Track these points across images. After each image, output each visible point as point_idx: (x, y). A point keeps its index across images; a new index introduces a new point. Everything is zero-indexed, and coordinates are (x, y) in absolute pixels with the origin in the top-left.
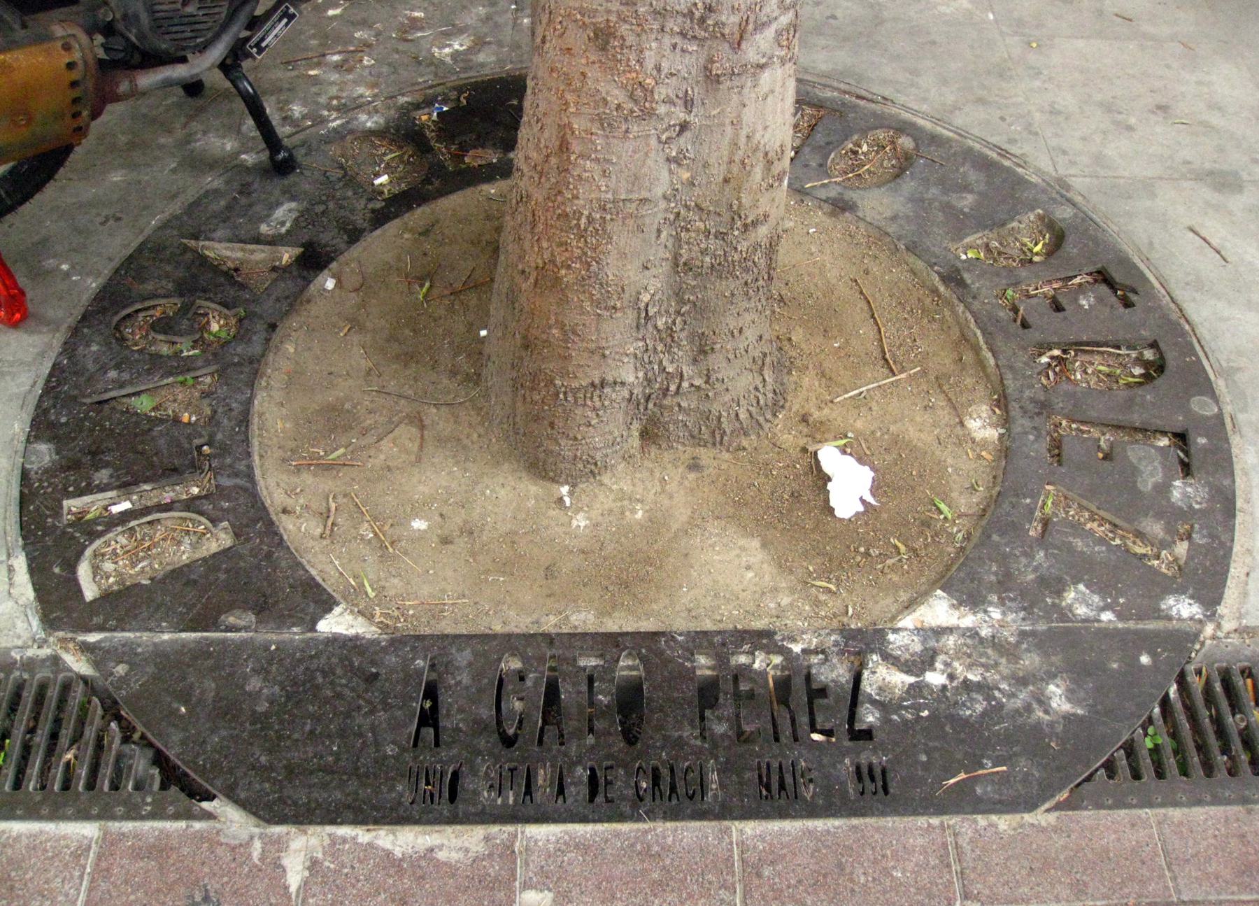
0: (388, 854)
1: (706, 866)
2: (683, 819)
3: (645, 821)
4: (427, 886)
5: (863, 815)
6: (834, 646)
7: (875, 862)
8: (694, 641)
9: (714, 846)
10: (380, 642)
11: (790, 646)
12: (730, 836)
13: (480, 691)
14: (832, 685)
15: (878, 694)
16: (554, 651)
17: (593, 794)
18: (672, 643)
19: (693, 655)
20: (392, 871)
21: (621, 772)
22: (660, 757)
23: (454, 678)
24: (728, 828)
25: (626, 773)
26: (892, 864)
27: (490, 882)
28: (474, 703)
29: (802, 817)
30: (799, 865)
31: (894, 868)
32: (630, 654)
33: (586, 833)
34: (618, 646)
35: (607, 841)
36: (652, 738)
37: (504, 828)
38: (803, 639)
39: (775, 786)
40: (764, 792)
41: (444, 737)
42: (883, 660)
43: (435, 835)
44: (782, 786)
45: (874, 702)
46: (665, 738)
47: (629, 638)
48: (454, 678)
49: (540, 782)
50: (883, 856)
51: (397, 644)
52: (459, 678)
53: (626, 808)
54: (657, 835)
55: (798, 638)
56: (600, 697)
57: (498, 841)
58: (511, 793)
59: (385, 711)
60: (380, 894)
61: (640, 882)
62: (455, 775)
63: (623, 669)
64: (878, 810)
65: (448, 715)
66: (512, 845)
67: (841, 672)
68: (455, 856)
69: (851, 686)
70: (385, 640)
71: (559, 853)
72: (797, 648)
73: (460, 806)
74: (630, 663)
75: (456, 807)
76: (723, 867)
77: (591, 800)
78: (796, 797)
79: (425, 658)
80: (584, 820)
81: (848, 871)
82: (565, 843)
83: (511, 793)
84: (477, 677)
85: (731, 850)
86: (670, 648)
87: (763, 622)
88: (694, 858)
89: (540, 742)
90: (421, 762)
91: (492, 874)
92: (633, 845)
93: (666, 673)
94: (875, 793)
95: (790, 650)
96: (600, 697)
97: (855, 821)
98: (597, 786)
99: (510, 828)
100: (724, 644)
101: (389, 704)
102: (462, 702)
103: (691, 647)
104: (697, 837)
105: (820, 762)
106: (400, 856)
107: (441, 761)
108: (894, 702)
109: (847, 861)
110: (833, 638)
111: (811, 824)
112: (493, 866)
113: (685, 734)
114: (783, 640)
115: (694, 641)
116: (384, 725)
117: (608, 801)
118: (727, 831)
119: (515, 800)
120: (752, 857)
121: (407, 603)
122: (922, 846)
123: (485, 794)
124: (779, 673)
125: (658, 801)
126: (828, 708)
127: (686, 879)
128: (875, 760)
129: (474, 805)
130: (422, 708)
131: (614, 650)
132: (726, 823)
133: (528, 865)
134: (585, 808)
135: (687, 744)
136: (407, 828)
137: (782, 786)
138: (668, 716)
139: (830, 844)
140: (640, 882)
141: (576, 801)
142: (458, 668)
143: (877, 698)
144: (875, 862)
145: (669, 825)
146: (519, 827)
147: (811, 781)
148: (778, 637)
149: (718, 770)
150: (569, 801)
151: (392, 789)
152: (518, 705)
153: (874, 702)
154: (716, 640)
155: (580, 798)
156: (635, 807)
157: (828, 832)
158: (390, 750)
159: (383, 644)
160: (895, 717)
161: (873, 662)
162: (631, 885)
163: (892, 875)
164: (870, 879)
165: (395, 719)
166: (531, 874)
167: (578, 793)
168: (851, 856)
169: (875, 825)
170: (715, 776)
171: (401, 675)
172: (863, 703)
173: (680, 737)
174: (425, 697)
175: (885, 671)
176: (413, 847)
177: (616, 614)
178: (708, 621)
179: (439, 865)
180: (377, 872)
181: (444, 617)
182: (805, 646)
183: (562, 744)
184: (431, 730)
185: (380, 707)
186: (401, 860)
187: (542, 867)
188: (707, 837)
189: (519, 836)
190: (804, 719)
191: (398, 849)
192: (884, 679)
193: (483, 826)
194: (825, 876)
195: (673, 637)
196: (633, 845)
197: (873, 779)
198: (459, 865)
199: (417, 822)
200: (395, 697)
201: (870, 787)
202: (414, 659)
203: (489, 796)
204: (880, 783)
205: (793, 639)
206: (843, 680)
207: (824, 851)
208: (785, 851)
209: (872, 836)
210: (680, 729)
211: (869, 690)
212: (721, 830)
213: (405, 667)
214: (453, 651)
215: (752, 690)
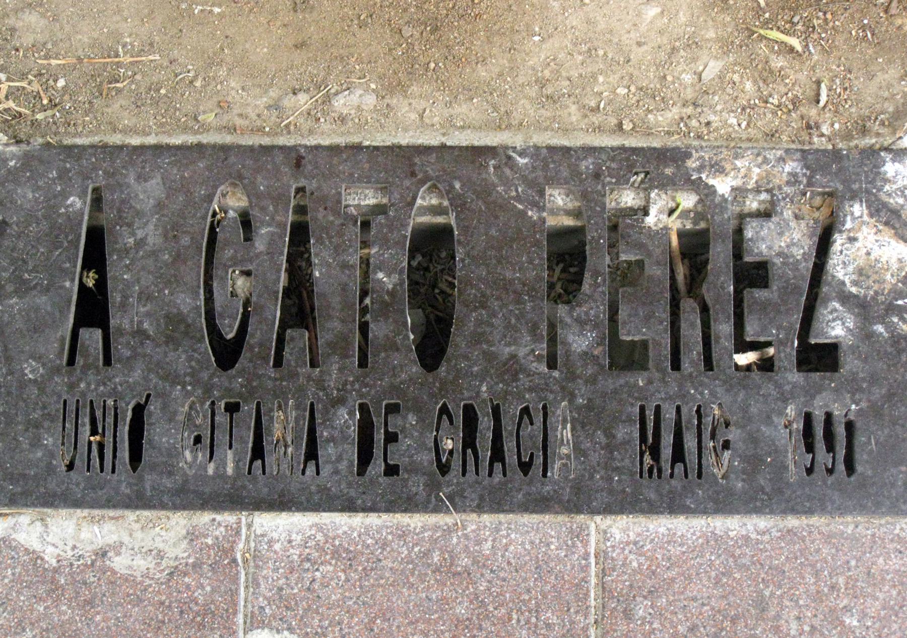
0: (36, 558)
1: (544, 596)
2: (511, 511)
3: (448, 511)
4: (98, 618)
5: (810, 512)
6: (788, 183)
7: (818, 597)
8: (545, 167)
9: (559, 560)
10: (5, 161)
11: (711, 182)
12: (586, 543)
13: (178, 258)
14: (778, 261)
15: (855, 283)
16: (302, 183)
17: (365, 457)
18: (508, 171)
19: (542, 193)
20: (42, 590)
21: (412, 419)
22: (478, 393)
23: (133, 234)
24: (583, 528)
25: (421, 420)
26: (845, 602)
27: (197, 614)
28: (168, 283)
29: (705, 512)
30: (694, 599)
31: (847, 609)
32: (434, 186)
33: (352, 529)
34: (413, 174)
35: (385, 545)
36: (466, 358)
37: (219, 518)
38: (735, 168)
39: (667, 452)
40: (648, 459)
41: (121, 349)
42: (871, 215)
43: (108, 526)
44: (679, 455)
45: (846, 298)
46: (490, 357)
47: (433, 158)
48: (133, 234)
49: (277, 433)
50: (833, 587)
51: (35, 163)
52: (140, 234)
53: (417, 485)
54: (466, 536)
55: (728, 167)
56: (380, 275)
57: (209, 541)
58: (230, 454)
59: (20, 298)
60: (24, 630)
61: (436, 622)
62: (139, 410)
63: (425, 210)
64: (833, 502)
65: (123, 306)
66: (232, 549)
67: (797, 236)
68: (142, 564)
69: (811, 265)
70: (14, 157)
71: (307, 565)
72: (723, 186)
73: (147, 477)
74: (434, 201)
75: (141, 479)
76: (570, 597)
77: (361, 472)
78: (700, 476)
79: (82, 195)
80: (350, 507)
81: (772, 613)
82: (319, 548)
83: (230, 454)
84: (171, 232)
85: (585, 568)
86: (507, 182)
87: (669, 115)
88: (525, 580)
89: (278, 363)
90: (83, 394)
91: (201, 600)
92: (427, 554)
93: (493, 232)
94: (830, 471)
95: (711, 190)
96: (380, 275)
97: (792, 522)
98: (371, 455)
99: (228, 518)
100: (597, 176)
101: (25, 282)
102: (147, 280)
103: (541, 180)
104: (532, 543)
105: (745, 409)
106: (54, 562)
107: (114, 393)
108: (881, 298)
109: (772, 594)
110: (788, 169)
111: (721, 524)
112: (202, 587)
113: (522, 352)
114: (700, 169)
115: (545, 167)
116: (19, 324)
117: (392, 471)
118: (580, 534)
119: (237, 467)
120: (618, 582)
121: (54, 62)
122: (897, 572)
123: (188, 454)
124: (689, 226)
125: (471, 475)
126: (764, 307)
127: (510, 619)
128: (838, 412)
129: (170, 474)
130: (82, 285)
131: (407, 183)
132: (581, 518)
133: (258, 585)
134: (350, 485)
135: (523, 370)
136: (63, 512)
137: (679, 455)
138: (494, 315)
139: (746, 561)
140: (436, 622)
141: (336, 472)
142: (139, 214)
143: (854, 290)
144: (818, 597)
145: (486, 518)
146: (244, 516)
147: (726, 445)
148: (692, 164)
149: (574, 421)
150: (326, 470)
151: (36, 443)
152: (241, 284)
153: (846, 298)
154: (583, 165)
155: (343, 466)
156: (433, 487)
157: (747, 538)
158: (31, 370)
159: (12, 163)
160: (880, 328)
161: (854, 219)
162: (421, 626)
163: (842, 623)
164: (807, 628)
165: (37, 310)
166: (262, 601)
167: (339, 459)
168: (780, 587)
169: (824, 529)
170: (568, 433)
171: (45, 225)
172: (827, 300)
173: (513, 357)
174: (86, 266)
175: (872, 238)
176: (74, 547)
177: (415, 89)
178: (573, 108)
179: (114, 580)
180: (19, 593)
181: (119, 91)
182: (738, 183)
183: (313, 365)
184: (98, 333)
185: (10, 288)
186: (56, 570)
187: (281, 589)
188: (548, 545)
189: (244, 530)
190: (724, 329)
191: (50, 549)
192: (868, 254)
193: (185, 513)
194: (734, 621)
195: (509, 158)
196: (427, 554)
197: (830, 447)
198: (148, 582)
199: (77, 504)
200: (35, 270)
201: (823, 456)
202: (65, 195)
203: (195, 458)
204: (841, 452)
205: (718, 169)
206: (798, 253)
207: (737, 576)
208: (672, 573)
209: (818, 551)
210: (515, 342)
211: (840, 273)
212: (571, 531)
213: (51, 209)
214: (131, 180)
215: (640, 264)
